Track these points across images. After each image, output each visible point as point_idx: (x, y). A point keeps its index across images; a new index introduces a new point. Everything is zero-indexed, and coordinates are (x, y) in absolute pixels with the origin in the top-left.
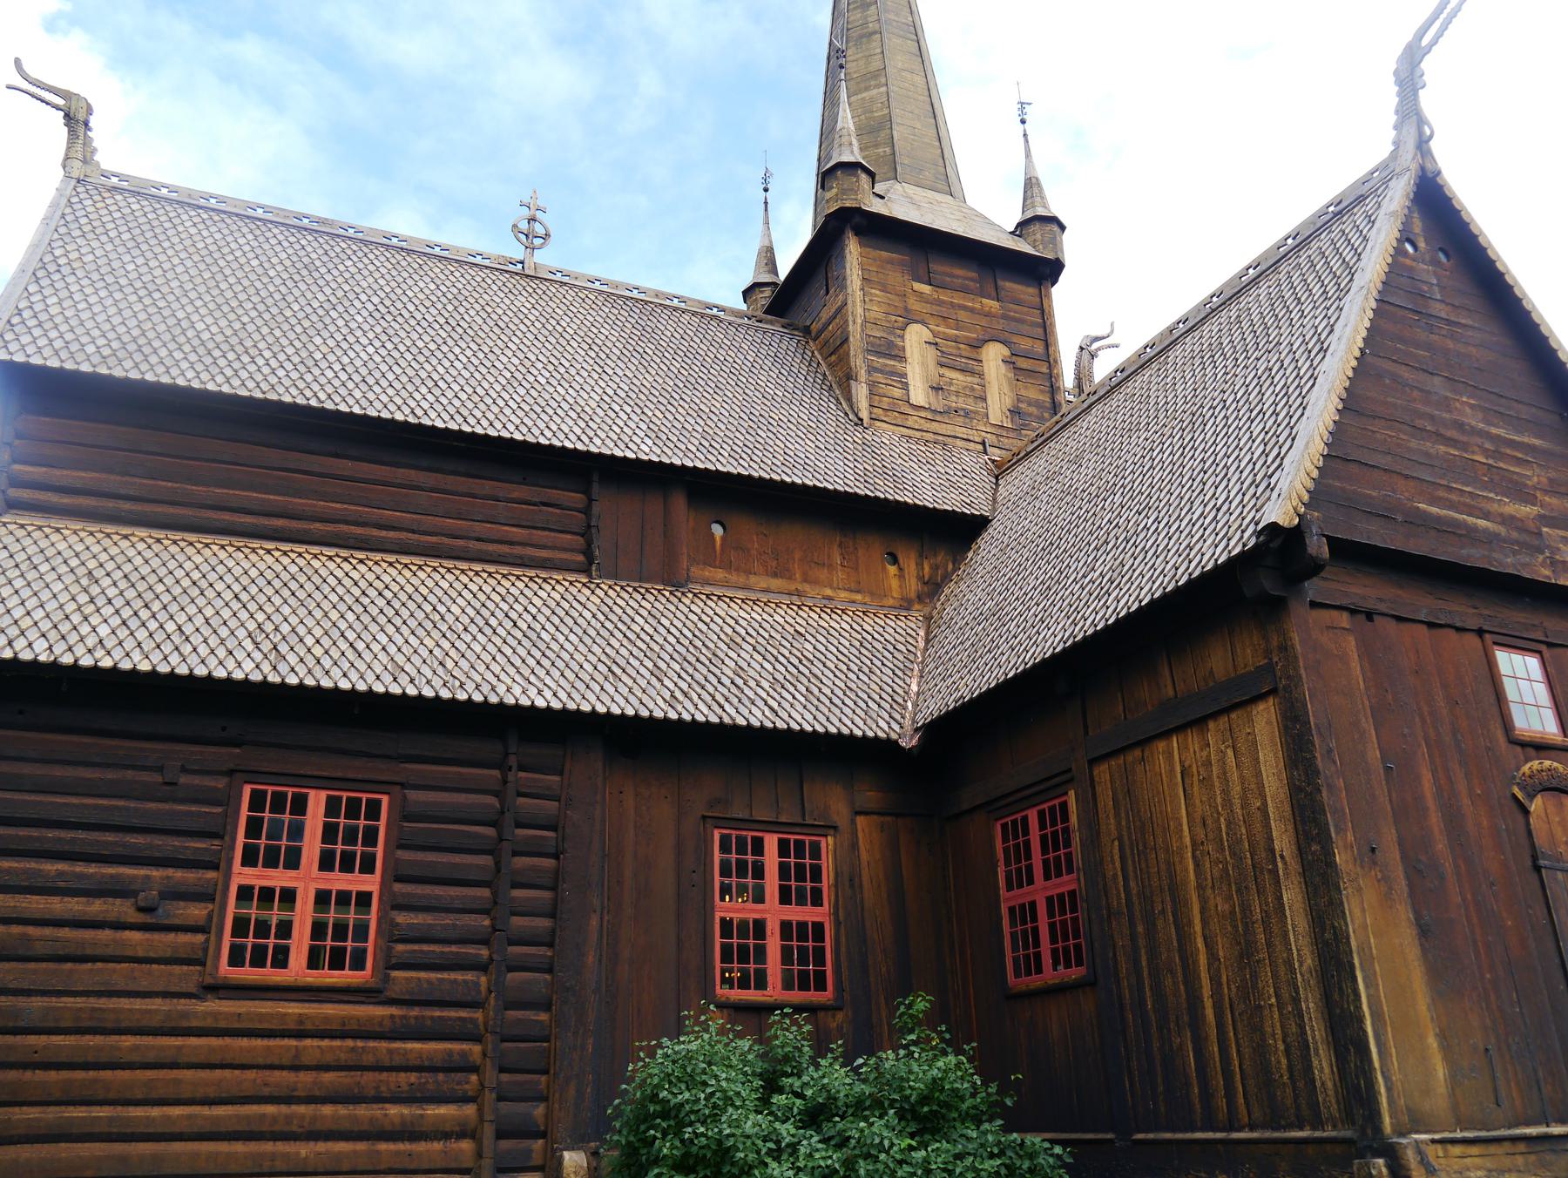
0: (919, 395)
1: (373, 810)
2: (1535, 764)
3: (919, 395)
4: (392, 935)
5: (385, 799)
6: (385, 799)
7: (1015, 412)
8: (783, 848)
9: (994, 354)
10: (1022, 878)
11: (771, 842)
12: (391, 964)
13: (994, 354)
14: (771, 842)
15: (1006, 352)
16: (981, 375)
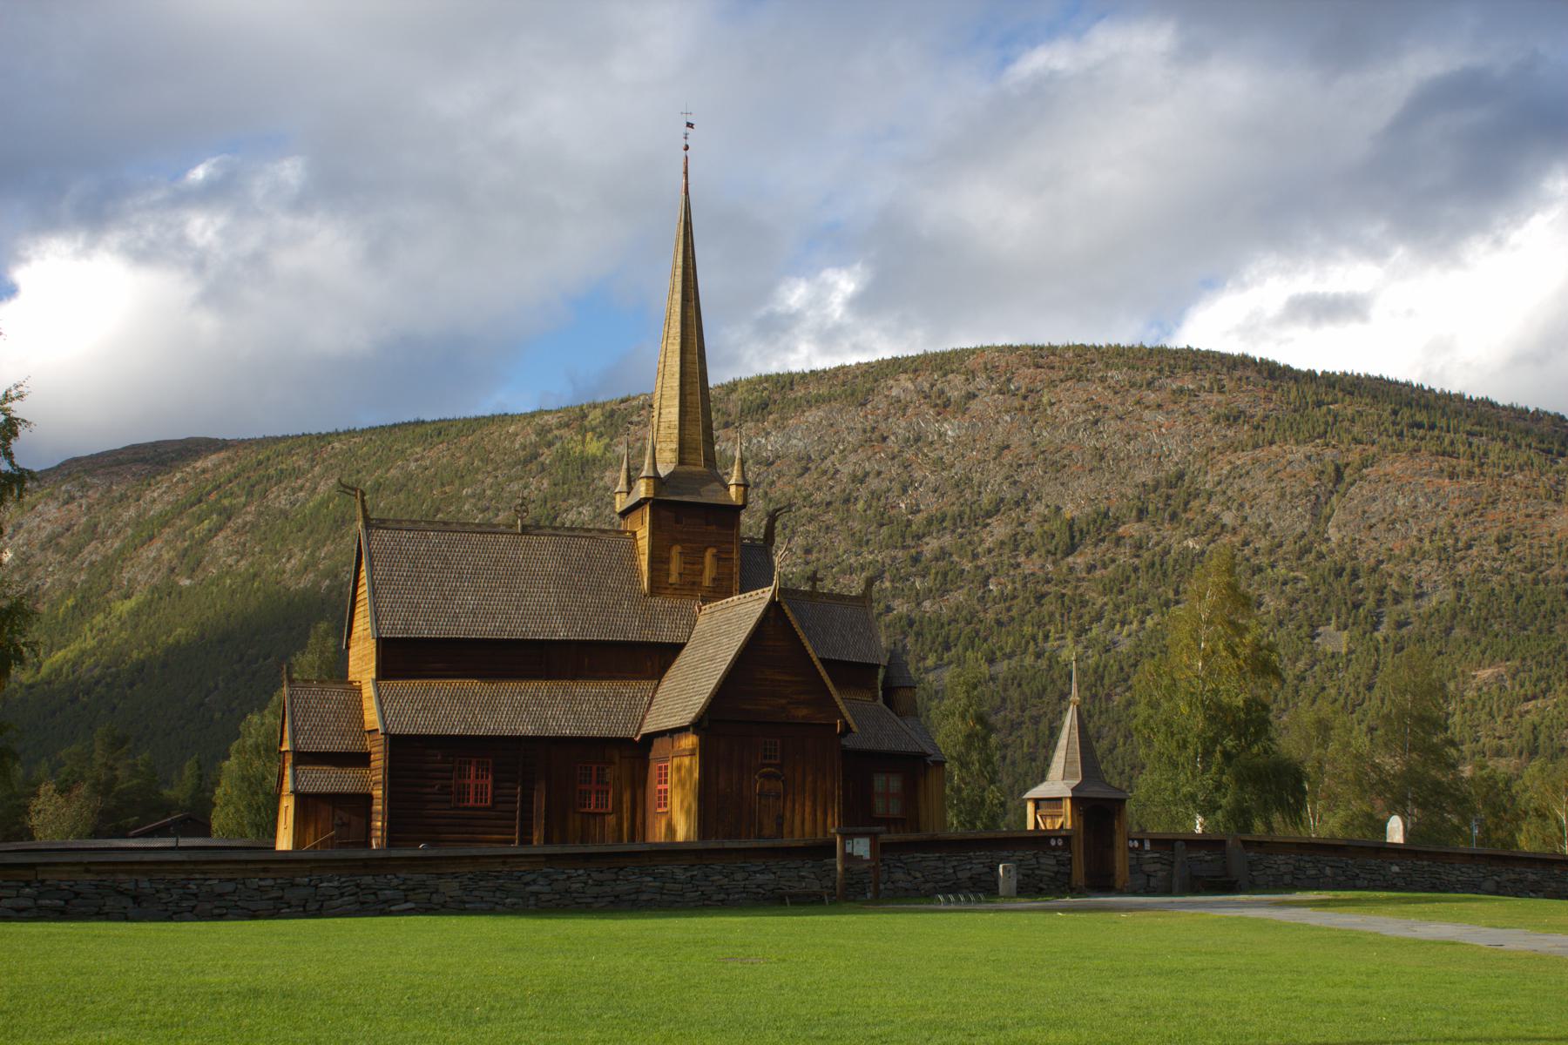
0: (674, 578)
1: (488, 763)
2: (765, 770)
3: (674, 578)
4: (494, 796)
5: (490, 761)
6: (490, 761)
7: (714, 579)
8: (598, 769)
9: (709, 556)
10: (660, 782)
11: (595, 767)
12: (494, 802)
13: (709, 556)
14: (595, 767)
15: (715, 551)
16: (703, 563)
